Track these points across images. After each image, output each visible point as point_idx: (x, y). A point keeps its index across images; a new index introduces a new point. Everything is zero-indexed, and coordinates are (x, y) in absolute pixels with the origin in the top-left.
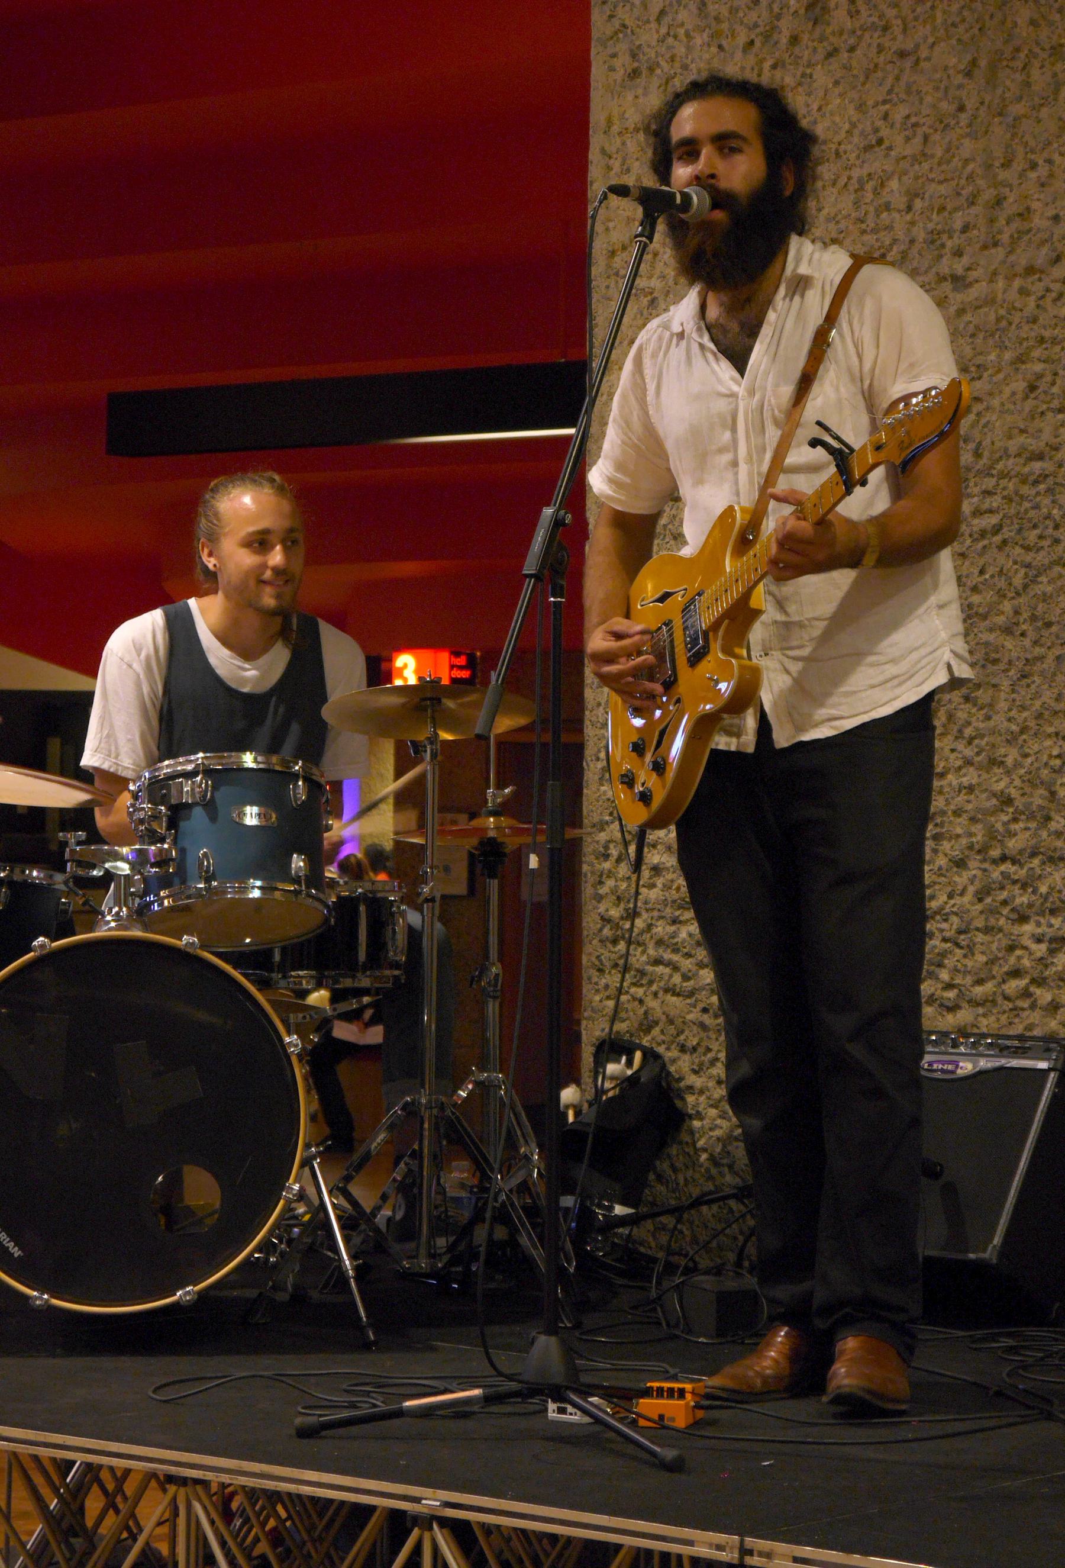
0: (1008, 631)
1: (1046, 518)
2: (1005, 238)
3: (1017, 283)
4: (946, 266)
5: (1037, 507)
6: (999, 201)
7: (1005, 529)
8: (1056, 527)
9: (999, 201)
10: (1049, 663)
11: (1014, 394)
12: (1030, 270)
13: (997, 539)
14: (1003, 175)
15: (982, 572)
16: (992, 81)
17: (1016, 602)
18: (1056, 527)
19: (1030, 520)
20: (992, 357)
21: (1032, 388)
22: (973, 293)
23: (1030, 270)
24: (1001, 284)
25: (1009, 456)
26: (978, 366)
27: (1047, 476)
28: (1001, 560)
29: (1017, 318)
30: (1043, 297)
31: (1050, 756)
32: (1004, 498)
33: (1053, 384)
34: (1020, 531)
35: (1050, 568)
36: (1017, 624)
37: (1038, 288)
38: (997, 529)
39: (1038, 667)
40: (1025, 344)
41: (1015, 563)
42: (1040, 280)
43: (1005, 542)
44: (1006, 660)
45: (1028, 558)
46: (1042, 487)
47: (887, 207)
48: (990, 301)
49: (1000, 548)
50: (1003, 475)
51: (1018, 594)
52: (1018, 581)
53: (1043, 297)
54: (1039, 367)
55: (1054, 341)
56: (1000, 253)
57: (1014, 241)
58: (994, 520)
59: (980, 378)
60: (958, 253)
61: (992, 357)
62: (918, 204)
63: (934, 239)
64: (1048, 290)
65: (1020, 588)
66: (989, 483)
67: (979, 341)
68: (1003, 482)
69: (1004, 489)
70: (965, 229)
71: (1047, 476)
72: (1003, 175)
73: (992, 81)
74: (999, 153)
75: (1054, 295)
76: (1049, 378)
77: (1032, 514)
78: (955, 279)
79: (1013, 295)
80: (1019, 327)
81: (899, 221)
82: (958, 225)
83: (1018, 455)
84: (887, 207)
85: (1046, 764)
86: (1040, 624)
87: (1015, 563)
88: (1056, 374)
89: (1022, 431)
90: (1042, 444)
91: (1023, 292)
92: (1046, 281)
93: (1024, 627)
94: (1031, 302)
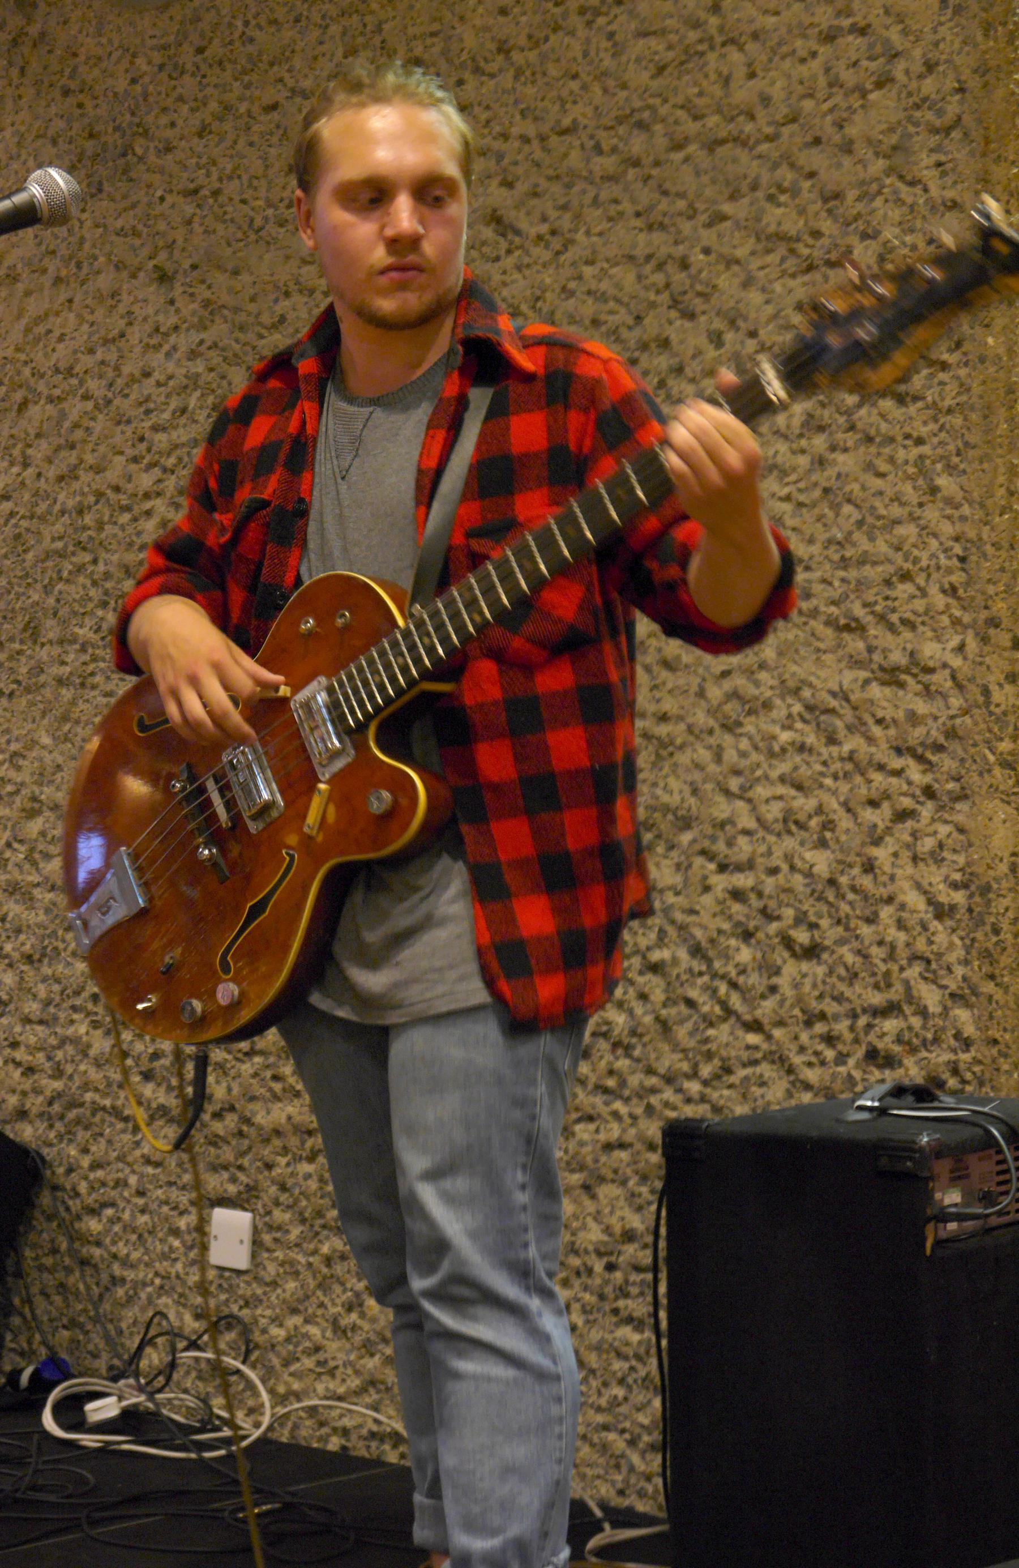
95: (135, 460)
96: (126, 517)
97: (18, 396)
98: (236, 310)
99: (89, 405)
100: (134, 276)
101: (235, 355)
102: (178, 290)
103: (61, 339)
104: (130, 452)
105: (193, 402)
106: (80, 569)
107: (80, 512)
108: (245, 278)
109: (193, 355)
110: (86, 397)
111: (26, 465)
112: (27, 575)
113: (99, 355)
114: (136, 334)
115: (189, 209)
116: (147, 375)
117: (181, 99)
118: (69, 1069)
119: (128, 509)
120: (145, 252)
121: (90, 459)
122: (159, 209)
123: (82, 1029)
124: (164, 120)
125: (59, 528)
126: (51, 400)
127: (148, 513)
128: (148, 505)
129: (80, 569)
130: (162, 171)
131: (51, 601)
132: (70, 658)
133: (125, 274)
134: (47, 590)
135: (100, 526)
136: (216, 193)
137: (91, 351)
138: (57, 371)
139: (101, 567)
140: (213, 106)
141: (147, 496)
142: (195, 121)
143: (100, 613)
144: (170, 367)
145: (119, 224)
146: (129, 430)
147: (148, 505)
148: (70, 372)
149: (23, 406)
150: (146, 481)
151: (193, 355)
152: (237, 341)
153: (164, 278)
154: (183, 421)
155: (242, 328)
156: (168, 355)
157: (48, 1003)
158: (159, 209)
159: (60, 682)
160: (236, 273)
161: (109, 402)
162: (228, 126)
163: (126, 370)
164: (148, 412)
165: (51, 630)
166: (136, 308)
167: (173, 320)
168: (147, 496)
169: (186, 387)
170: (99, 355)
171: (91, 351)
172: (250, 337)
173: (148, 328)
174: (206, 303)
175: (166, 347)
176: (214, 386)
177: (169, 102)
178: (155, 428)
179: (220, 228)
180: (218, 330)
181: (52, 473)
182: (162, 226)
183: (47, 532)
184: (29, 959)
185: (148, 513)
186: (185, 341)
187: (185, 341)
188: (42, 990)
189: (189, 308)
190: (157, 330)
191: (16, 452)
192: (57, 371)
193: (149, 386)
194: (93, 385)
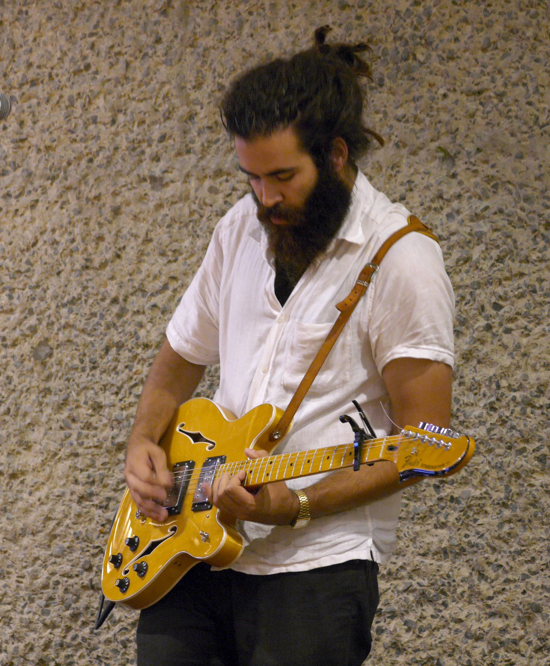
2: (197, 146)
3: (207, 183)
4: (146, 168)
6: (191, 117)
9: (191, 117)
12: (219, 173)
14: (194, 95)
16: (184, 18)
20: (187, 243)
22: (169, 192)
23: (219, 173)
24: (193, 183)
26: (174, 251)
29: (207, 211)
30: (230, 195)
37: (226, 187)
42: (227, 181)
47: (95, 120)
48: (185, 198)
56: (192, 159)
57: (205, 150)
59: (176, 260)
60: (156, 159)
61: (187, 243)
62: (121, 118)
63: (134, 147)
64: (234, 189)
70: (163, 138)
72: (194, 95)
73: (184, 18)
74: (191, 77)
78: (153, 179)
79: (204, 193)
81: (105, 132)
82: (156, 135)
84: (95, 120)
91: (213, 190)
92: (233, 182)
94: (220, 198)
98: (522, 186)
100: (414, 153)
101: (520, 219)
102: (460, 167)
108: (528, 161)
109: (476, 217)
115: (472, 105)
117: (465, 20)
120: (427, 135)
122: (442, 103)
124: (447, 36)
130: (446, 74)
133: (404, 152)
136: (500, 96)
140: (498, 28)
142: (481, 38)
144: (454, 226)
145: (400, 112)
151: (476, 217)
152: (523, 209)
153: (448, 157)
154: (466, 267)
155: (527, 199)
156: (450, 216)
158: (442, 103)
160: (520, 157)
162: (512, 44)
166: (417, 179)
167: (456, 189)
169: (469, 242)
172: (537, 206)
173: (430, 194)
174: (489, 179)
175: (447, 210)
176: (499, 242)
177: (452, 22)
179: (505, 123)
180: (501, 199)
182: (444, 117)
186: (467, 208)
187: (467, 208)
189: (470, 182)
190: (440, 197)
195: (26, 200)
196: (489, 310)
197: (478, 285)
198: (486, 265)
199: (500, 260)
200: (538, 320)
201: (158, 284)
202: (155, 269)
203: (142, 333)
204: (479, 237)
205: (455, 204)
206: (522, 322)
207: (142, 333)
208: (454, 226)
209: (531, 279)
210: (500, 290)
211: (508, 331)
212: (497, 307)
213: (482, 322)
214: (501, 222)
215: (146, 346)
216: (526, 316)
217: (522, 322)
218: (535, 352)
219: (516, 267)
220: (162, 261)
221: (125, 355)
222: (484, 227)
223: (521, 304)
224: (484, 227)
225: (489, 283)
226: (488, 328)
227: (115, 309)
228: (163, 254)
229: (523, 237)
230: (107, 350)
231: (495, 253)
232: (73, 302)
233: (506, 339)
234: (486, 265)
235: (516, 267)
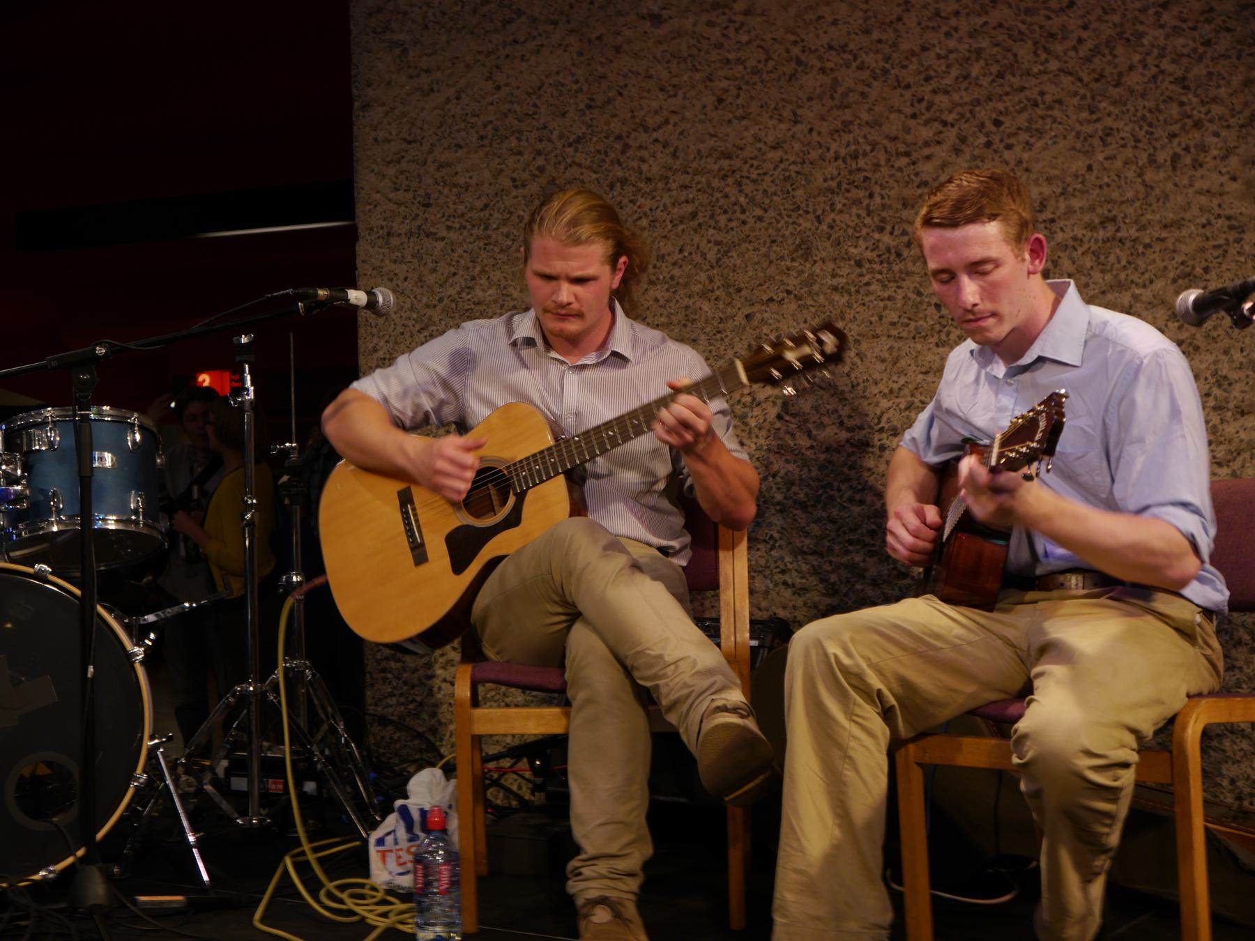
0: (703, 294)
1: (735, 204)
5: (726, 196)
7: (700, 215)
8: (743, 211)
10: (740, 319)
11: (704, 107)
13: (694, 224)
15: (681, 251)
17: (710, 273)
18: (743, 211)
19: (721, 207)
20: (685, 78)
21: (720, 101)
25: (701, 158)
26: (674, 86)
27: (734, 172)
28: (697, 239)
30: (726, 28)
31: (742, 395)
32: (699, 190)
33: (738, 96)
34: (712, 217)
35: (739, 245)
36: (713, 291)
38: (694, 215)
39: (730, 325)
40: (713, 66)
41: (709, 242)
42: (724, 14)
43: (700, 225)
44: (703, 319)
45: (719, 237)
46: (730, 180)
49: (696, 231)
50: (697, 172)
51: (712, 267)
52: (711, 256)
53: (726, 28)
54: (725, 84)
55: (740, 61)
58: (689, 208)
59: (675, 96)
61: (685, 78)
64: (731, 21)
65: (714, 262)
66: (686, 179)
67: (673, 66)
68: (697, 178)
69: (698, 183)
71: (734, 172)
75: (737, 25)
76: (734, 91)
77: (722, 202)
80: (707, 52)
83: (710, 155)
85: (739, 401)
86: (731, 290)
87: (709, 242)
88: (740, 88)
89: (712, 136)
90: (730, 145)
93: (718, 293)
95: (914, 116)
96: (903, 161)
97: (789, 69)
99: (865, 75)
101: (1020, 32)
103: (835, 23)
104: (909, 111)
105: (975, 71)
106: (857, 202)
107: (855, 157)
109: (973, 34)
110: (861, 68)
111: (796, 122)
112: (799, 208)
113: (875, 35)
114: (911, 20)
116: (924, 49)
118: (844, 589)
119: (907, 154)
121: (865, 117)
123: (858, 558)
125: (831, 170)
126: (823, 71)
127: (928, 158)
128: (926, 152)
129: (857, 202)
131: (824, 227)
132: (845, 271)
134: (819, 220)
135: (877, 166)
137: (867, 32)
138: (831, 48)
139: (878, 200)
141: (927, 144)
143: (877, 236)
144: (952, 43)
146: (908, 94)
147: (926, 152)
148: (844, 48)
149: (792, 77)
150: (926, 133)
151: (973, 34)
152: (1023, 22)
154: (965, 85)
157: (822, 538)
159: (835, 289)
161: (885, 72)
163: (905, 46)
164: (928, 79)
165: (824, 249)
168: (927, 144)
169: (969, 59)
170: (875, 35)
171: (867, 32)
175: (945, 29)
176: (999, 57)
178: (935, 92)
181: (824, 127)
183: (819, 176)
184: (803, 506)
185: (928, 158)
188: (815, 529)
190: (938, 15)
191: (786, 113)
192: (831, 48)
193: (929, 58)
194: (869, 59)
195: (531, 45)
196: (990, 127)
197: (977, 102)
198: (985, 82)
199: (1000, 75)
200: (1040, 133)
201: (658, 119)
202: (655, 105)
203: (645, 167)
204: (979, 52)
205: (953, 22)
206: (1024, 136)
207: (645, 167)
208: (952, 43)
209: (1033, 93)
210: (1000, 106)
211: (1009, 147)
212: (997, 123)
213: (982, 140)
214: (1001, 37)
215: (649, 180)
216: (1028, 129)
217: (1024, 136)
218: (1036, 167)
219: (1016, 81)
220: (661, 96)
221: (629, 189)
222: (984, 43)
223: (1022, 120)
224: (984, 43)
225: (990, 99)
226: (988, 144)
227: (618, 146)
228: (662, 90)
229: (1024, 51)
230: (612, 186)
231: (995, 69)
232: (578, 140)
233: (1007, 155)
234: (985, 82)
235: (1016, 81)
